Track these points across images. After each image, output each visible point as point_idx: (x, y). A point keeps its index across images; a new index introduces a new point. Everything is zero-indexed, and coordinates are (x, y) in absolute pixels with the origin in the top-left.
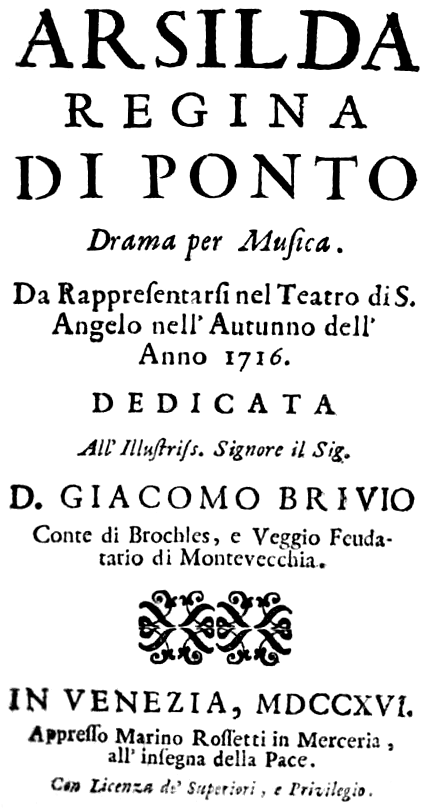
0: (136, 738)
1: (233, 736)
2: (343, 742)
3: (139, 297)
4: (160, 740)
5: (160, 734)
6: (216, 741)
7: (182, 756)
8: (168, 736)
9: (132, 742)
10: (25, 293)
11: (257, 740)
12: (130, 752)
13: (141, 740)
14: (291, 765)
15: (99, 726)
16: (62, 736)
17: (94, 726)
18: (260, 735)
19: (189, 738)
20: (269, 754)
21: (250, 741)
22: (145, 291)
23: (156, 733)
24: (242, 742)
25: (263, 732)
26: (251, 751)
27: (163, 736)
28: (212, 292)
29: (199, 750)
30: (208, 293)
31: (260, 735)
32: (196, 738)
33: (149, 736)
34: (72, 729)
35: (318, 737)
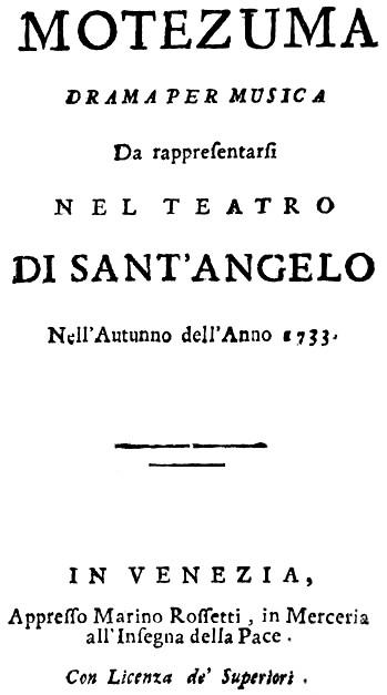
1: (210, 614)
4: (141, 619)
6: (192, 618)
7: (160, 634)
12: (109, 631)
13: (121, 619)
14: (267, 641)
19: (168, 616)
24: (219, 619)
27: (144, 615)
29: (177, 628)
31: (235, 613)
32: (174, 616)
33: (129, 615)
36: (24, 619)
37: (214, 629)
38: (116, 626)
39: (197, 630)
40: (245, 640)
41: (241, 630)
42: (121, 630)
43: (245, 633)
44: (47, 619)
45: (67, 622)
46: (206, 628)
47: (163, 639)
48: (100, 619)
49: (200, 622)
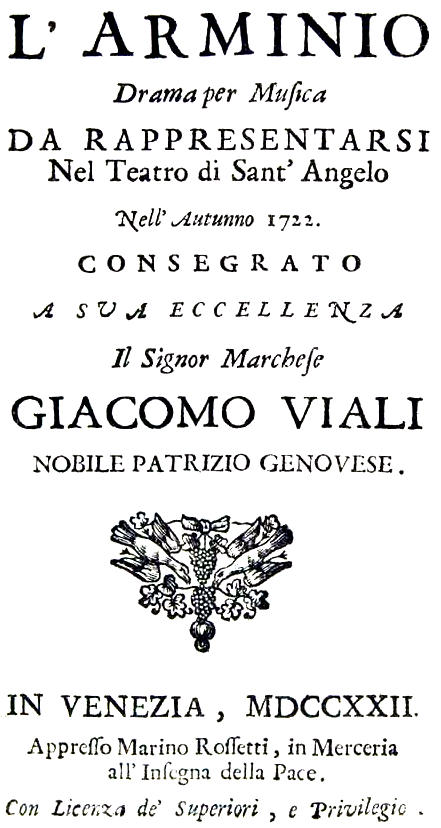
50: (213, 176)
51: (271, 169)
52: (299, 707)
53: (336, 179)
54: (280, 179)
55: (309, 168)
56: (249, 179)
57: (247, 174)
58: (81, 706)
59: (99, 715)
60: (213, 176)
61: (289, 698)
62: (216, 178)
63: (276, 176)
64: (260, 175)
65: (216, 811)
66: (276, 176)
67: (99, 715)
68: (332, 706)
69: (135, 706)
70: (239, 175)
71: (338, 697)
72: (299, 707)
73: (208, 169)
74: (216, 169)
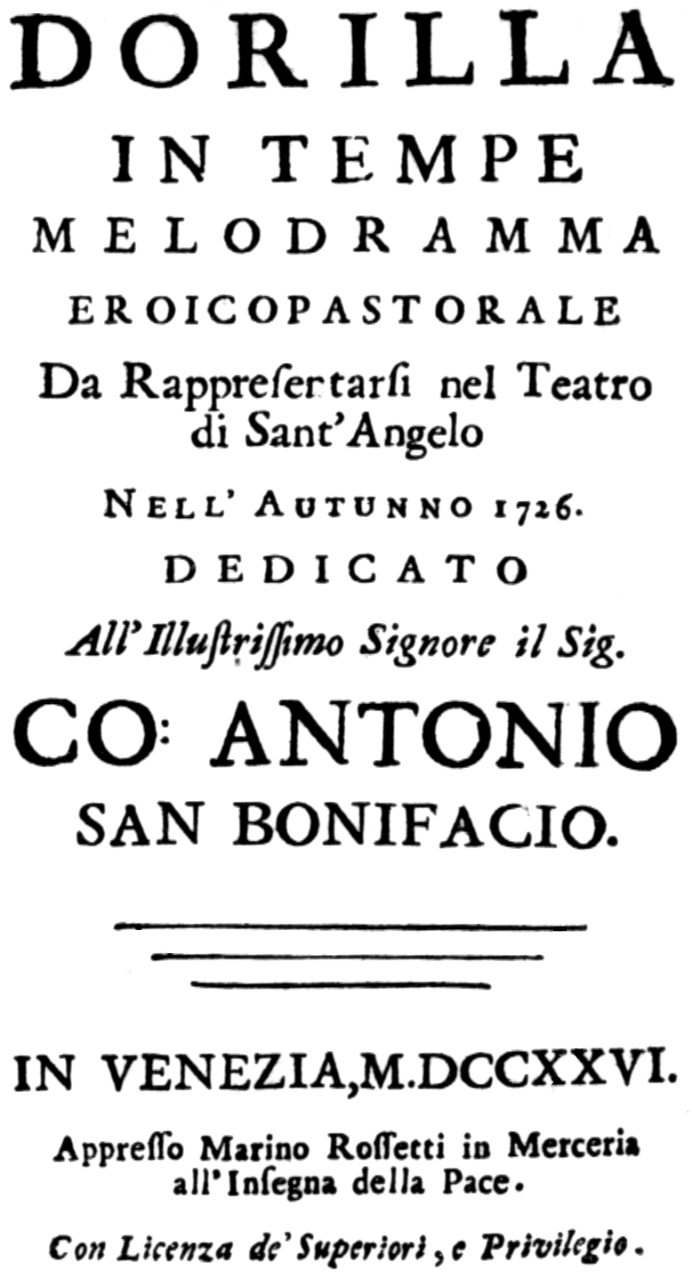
0: (234, 1151)
1: (393, 1142)
2: (582, 1148)
3: (259, 389)
5: (274, 1143)
6: (365, 1150)
8: (287, 1145)
9: (227, 1158)
10: (61, 381)
11: (431, 1149)
13: (241, 1155)
15: (169, 1134)
16: (108, 1151)
17: (160, 1135)
18: (436, 1141)
19: (320, 1147)
20: (448, 1172)
21: (420, 1151)
22: (270, 378)
23: (265, 1142)
25: (441, 1136)
26: (418, 1167)
28: (382, 379)
30: (375, 380)
31: (436, 1141)
32: (334, 1147)
33: (256, 1147)
34: (123, 1142)
35: (541, 1141)
36: (79, 1151)
37: (394, 1170)
38: (225, 1168)
39: (365, 1170)
40: (453, 1187)
41: (448, 1172)
42: (233, 1174)
43: (453, 1177)
44: (116, 1154)
45: (151, 1157)
46: (378, 1167)
47: (302, 1186)
48: (210, 1153)
49: (378, 1157)
50: (216, 438)
51: (308, 429)
52: (460, 1071)
53: (401, 443)
54: (324, 443)
55: (361, 426)
56: (275, 443)
57: (271, 436)
58: (138, 1071)
59: (166, 1087)
60: (216, 438)
61: (441, 1056)
62: (223, 444)
63: (316, 437)
64: (291, 438)
65: (361, 1252)
66: (316, 437)
67: (166, 1087)
68: (514, 1069)
69: (229, 1071)
70: (256, 437)
71: (524, 1056)
72: (460, 1071)
73: (208, 429)
74: (223, 430)
